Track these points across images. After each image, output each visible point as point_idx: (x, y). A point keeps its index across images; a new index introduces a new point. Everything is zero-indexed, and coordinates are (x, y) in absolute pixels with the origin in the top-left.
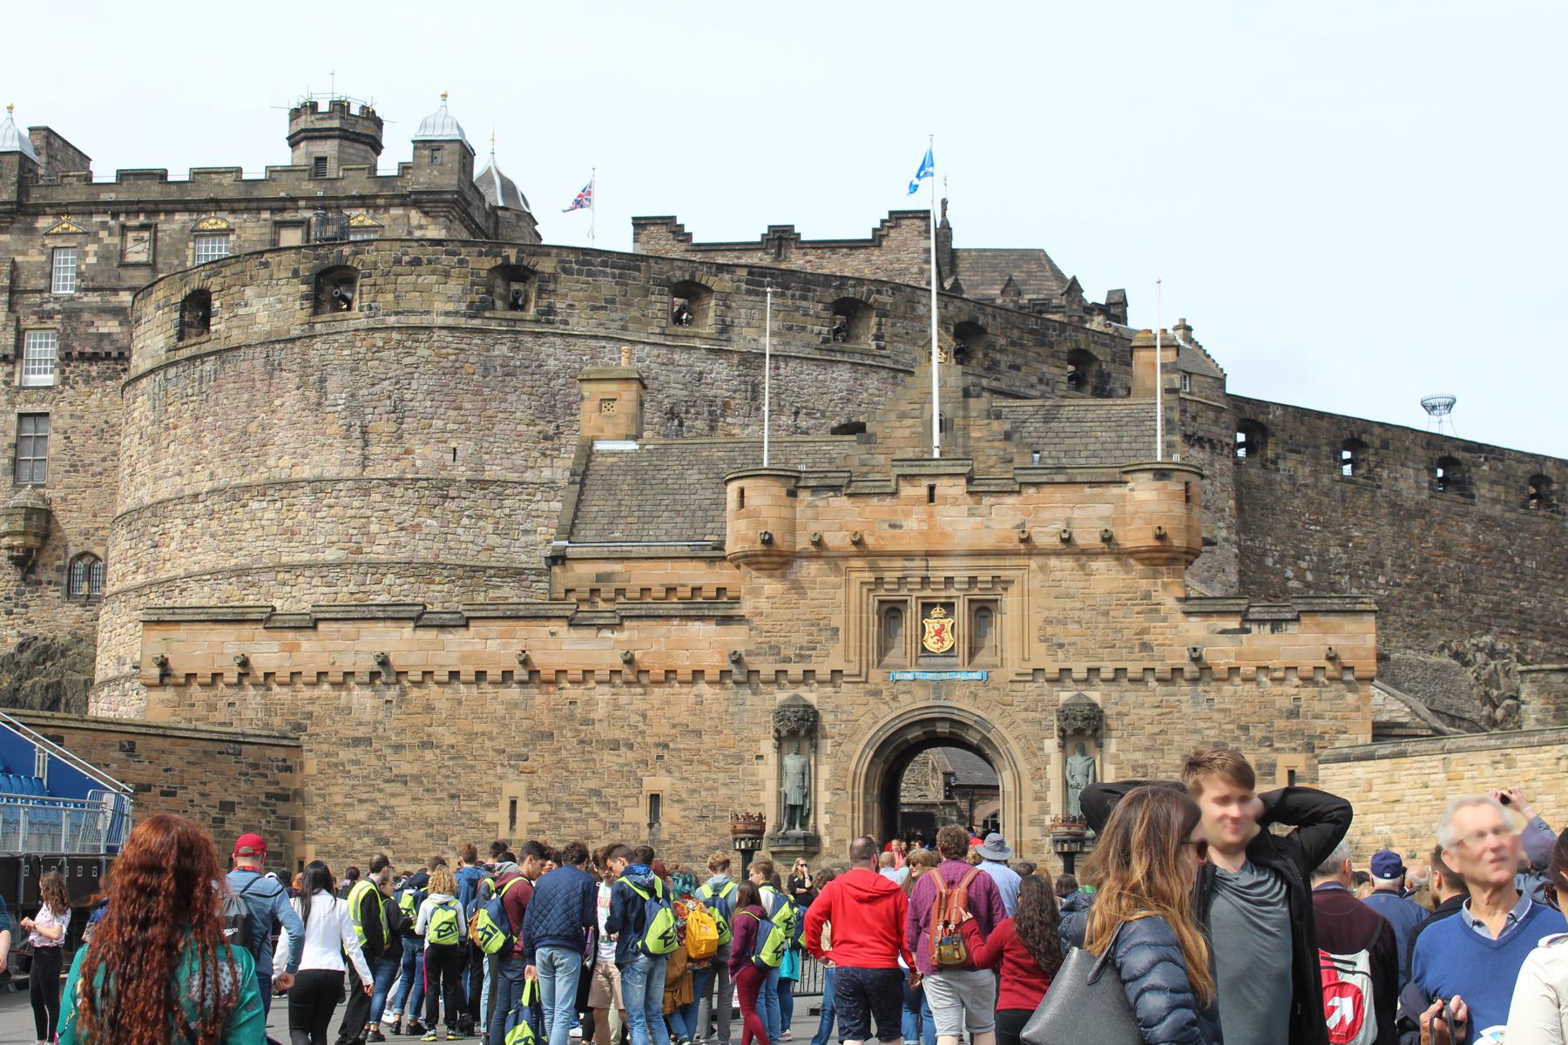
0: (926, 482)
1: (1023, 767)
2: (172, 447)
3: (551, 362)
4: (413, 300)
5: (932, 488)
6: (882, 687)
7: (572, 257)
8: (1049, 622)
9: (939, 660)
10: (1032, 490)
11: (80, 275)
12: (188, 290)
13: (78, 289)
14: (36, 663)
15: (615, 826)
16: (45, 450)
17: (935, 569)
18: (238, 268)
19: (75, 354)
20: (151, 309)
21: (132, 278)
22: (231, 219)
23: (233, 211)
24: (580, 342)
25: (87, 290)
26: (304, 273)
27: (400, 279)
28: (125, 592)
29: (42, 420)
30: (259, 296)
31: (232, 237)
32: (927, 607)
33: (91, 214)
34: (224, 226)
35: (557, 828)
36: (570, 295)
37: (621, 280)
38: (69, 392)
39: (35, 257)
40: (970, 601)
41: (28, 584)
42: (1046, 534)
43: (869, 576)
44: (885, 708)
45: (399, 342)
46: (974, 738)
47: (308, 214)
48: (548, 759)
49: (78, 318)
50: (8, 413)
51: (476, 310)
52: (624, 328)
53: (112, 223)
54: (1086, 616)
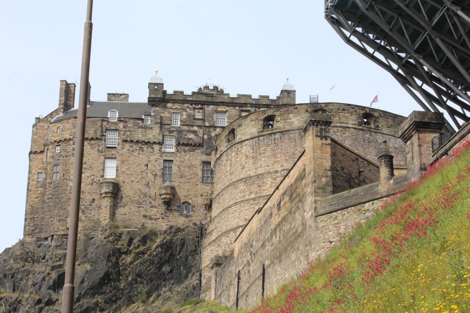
2: (263, 159)
3: (379, 140)
4: (343, 120)
7: (382, 113)
11: (181, 121)
12: (266, 115)
13: (181, 125)
14: (176, 232)
16: (171, 171)
18: (286, 109)
19: (181, 143)
20: (248, 121)
21: (197, 123)
22: (227, 108)
23: (227, 106)
24: (386, 136)
25: (184, 125)
26: (310, 110)
27: (340, 114)
28: (247, 200)
29: (170, 163)
30: (295, 117)
31: (227, 113)
33: (184, 103)
34: (225, 110)
36: (382, 123)
37: (393, 121)
38: (179, 154)
39: (167, 114)
41: (168, 210)
45: (341, 131)
47: (250, 109)
49: (182, 133)
50: (161, 159)
51: (360, 124)
52: (395, 134)
53: (190, 107)
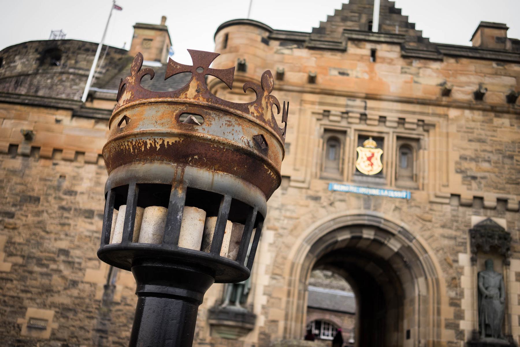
0: (369, 46)
1: (442, 275)
5: (373, 53)
6: (320, 194)
8: (463, 158)
9: (370, 179)
10: (452, 61)
15: (74, 283)
17: (372, 109)
32: (362, 138)
35: (23, 279)
40: (399, 138)
42: (463, 92)
43: (320, 109)
44: (322, 211)
46: (394, 245)
48: (31, 219)
54: (494, 158)
